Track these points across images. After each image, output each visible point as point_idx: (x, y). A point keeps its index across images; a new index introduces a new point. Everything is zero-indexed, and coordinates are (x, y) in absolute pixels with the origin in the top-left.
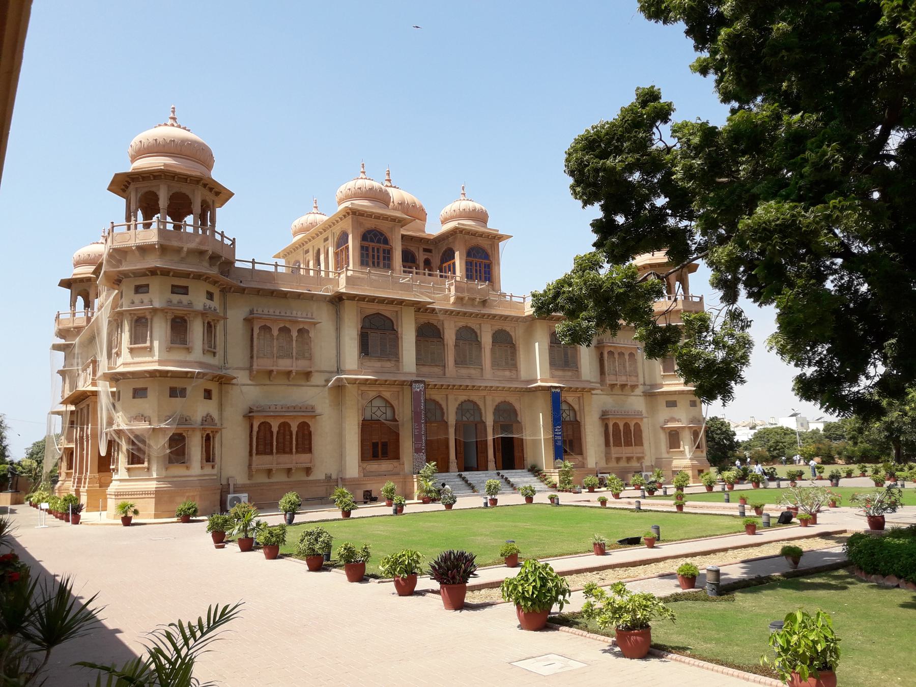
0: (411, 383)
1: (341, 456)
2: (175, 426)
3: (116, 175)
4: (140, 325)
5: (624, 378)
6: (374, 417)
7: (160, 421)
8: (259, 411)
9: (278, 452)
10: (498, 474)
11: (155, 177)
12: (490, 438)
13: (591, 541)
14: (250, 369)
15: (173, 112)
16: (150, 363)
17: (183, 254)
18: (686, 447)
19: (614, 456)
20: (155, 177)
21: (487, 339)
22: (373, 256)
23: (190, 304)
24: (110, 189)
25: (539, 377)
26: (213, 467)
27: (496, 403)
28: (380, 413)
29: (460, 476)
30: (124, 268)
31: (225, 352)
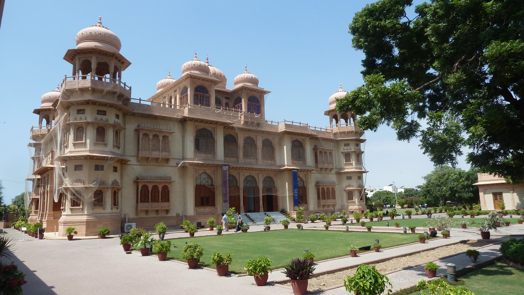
0: (221, 166)
1: (185, 204)
2: (98, 186)
3: (69, 51)
4: (80, 131)
5: (327, 165)
6: (202, 184)
7: (89, 183)
8: (142, 179)
9: (152, 201)
10: (265, 214)
11: (90, 52)
12: (261, 195)
13: (349, 249)
14: (137, 156)
15: (100, 20)
16: (84, 151)
17: (104, 94)
18: (356, 200)
19: (322, 204)
20: (90, 52)
22: (201, 99)
23: (107, 120)
24: (65, 58)
25: (286, 164)
26: (117, 208)
28: (205, 181)
29: (246, 215)
30: (72, 100)
31: (124, 147)
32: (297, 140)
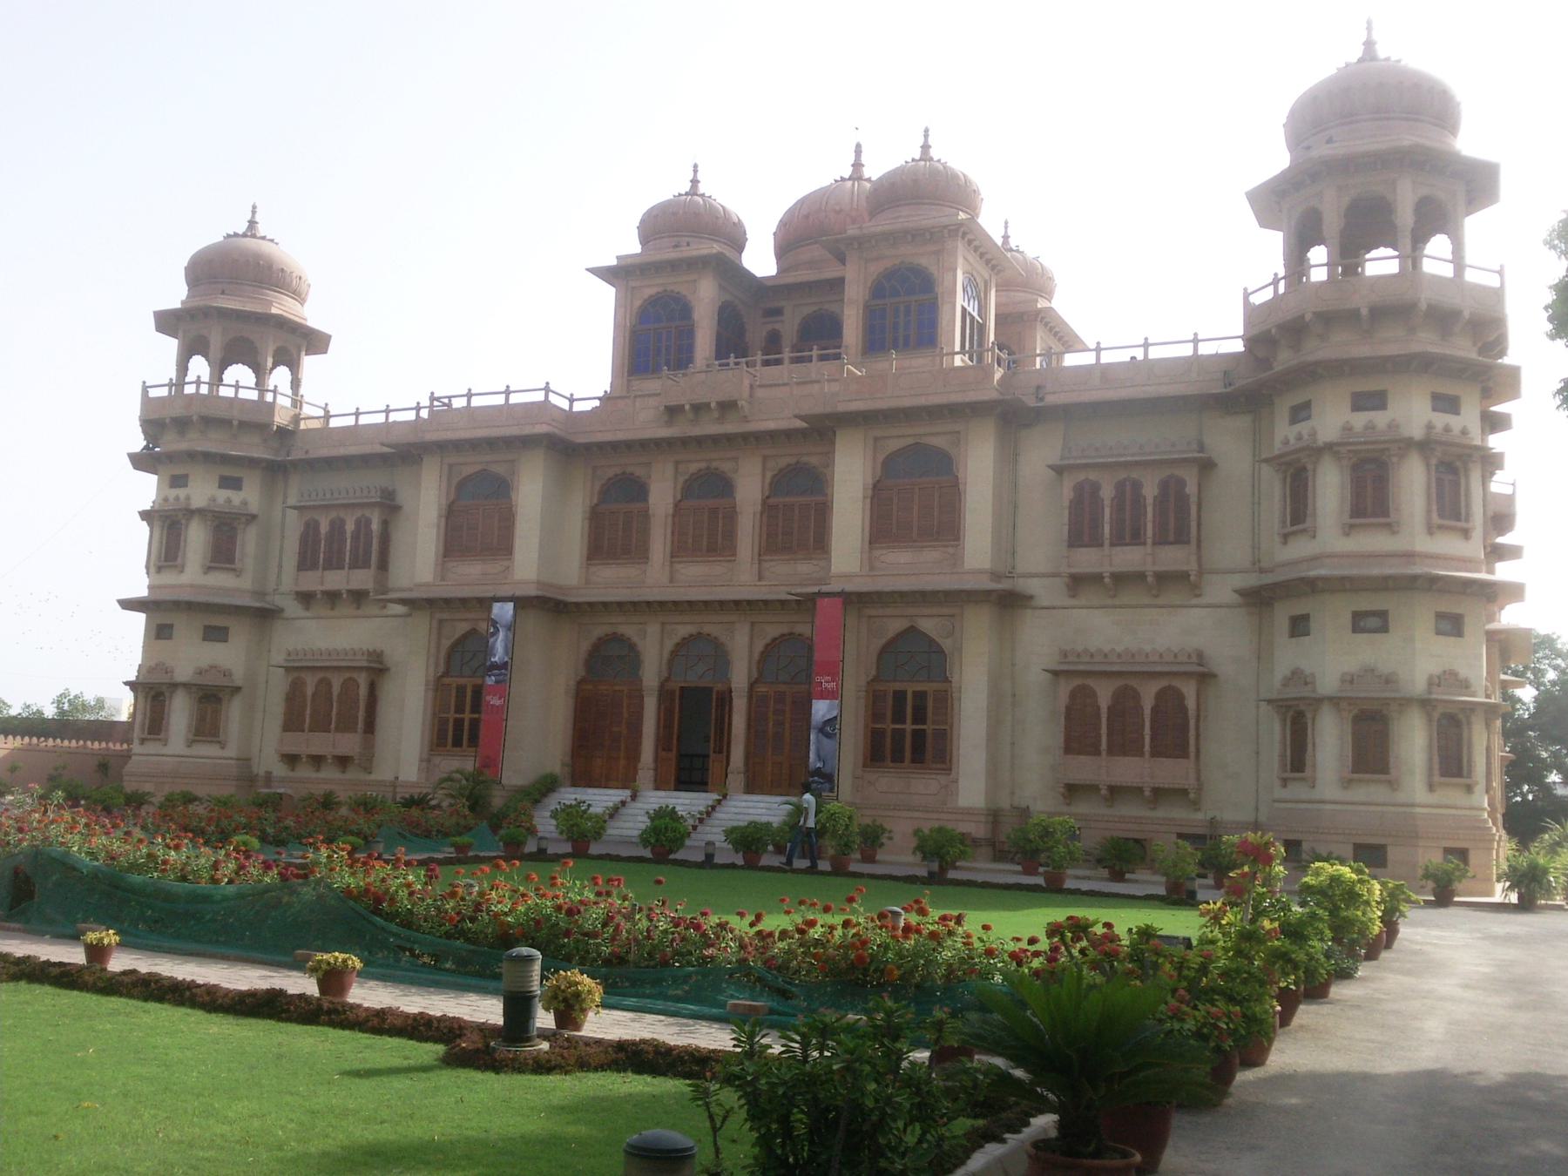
27: (768, 640)
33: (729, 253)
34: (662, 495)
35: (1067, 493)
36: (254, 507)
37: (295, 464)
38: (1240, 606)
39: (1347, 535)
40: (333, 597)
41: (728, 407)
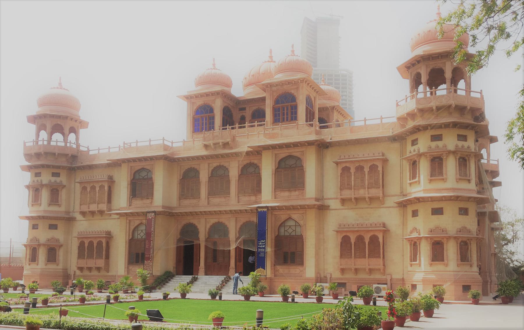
6: (139, 237)
21: (234, 173)
27: (241, 223)
32: (290, 157)
33: (226, 89)
34: (204, 176)
35: (340, 171)
36: (64, 183)
37: (79, 168)
38: (396, 207)
39: (430, 183)
40: (93, 213)
41: (226, 145)
